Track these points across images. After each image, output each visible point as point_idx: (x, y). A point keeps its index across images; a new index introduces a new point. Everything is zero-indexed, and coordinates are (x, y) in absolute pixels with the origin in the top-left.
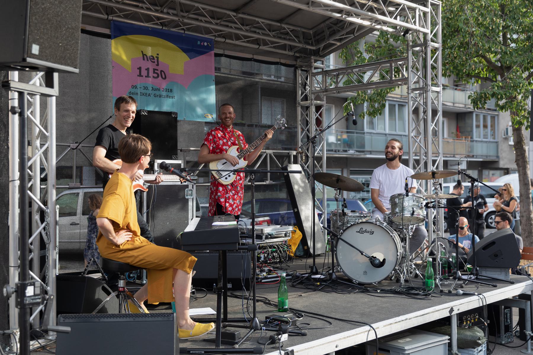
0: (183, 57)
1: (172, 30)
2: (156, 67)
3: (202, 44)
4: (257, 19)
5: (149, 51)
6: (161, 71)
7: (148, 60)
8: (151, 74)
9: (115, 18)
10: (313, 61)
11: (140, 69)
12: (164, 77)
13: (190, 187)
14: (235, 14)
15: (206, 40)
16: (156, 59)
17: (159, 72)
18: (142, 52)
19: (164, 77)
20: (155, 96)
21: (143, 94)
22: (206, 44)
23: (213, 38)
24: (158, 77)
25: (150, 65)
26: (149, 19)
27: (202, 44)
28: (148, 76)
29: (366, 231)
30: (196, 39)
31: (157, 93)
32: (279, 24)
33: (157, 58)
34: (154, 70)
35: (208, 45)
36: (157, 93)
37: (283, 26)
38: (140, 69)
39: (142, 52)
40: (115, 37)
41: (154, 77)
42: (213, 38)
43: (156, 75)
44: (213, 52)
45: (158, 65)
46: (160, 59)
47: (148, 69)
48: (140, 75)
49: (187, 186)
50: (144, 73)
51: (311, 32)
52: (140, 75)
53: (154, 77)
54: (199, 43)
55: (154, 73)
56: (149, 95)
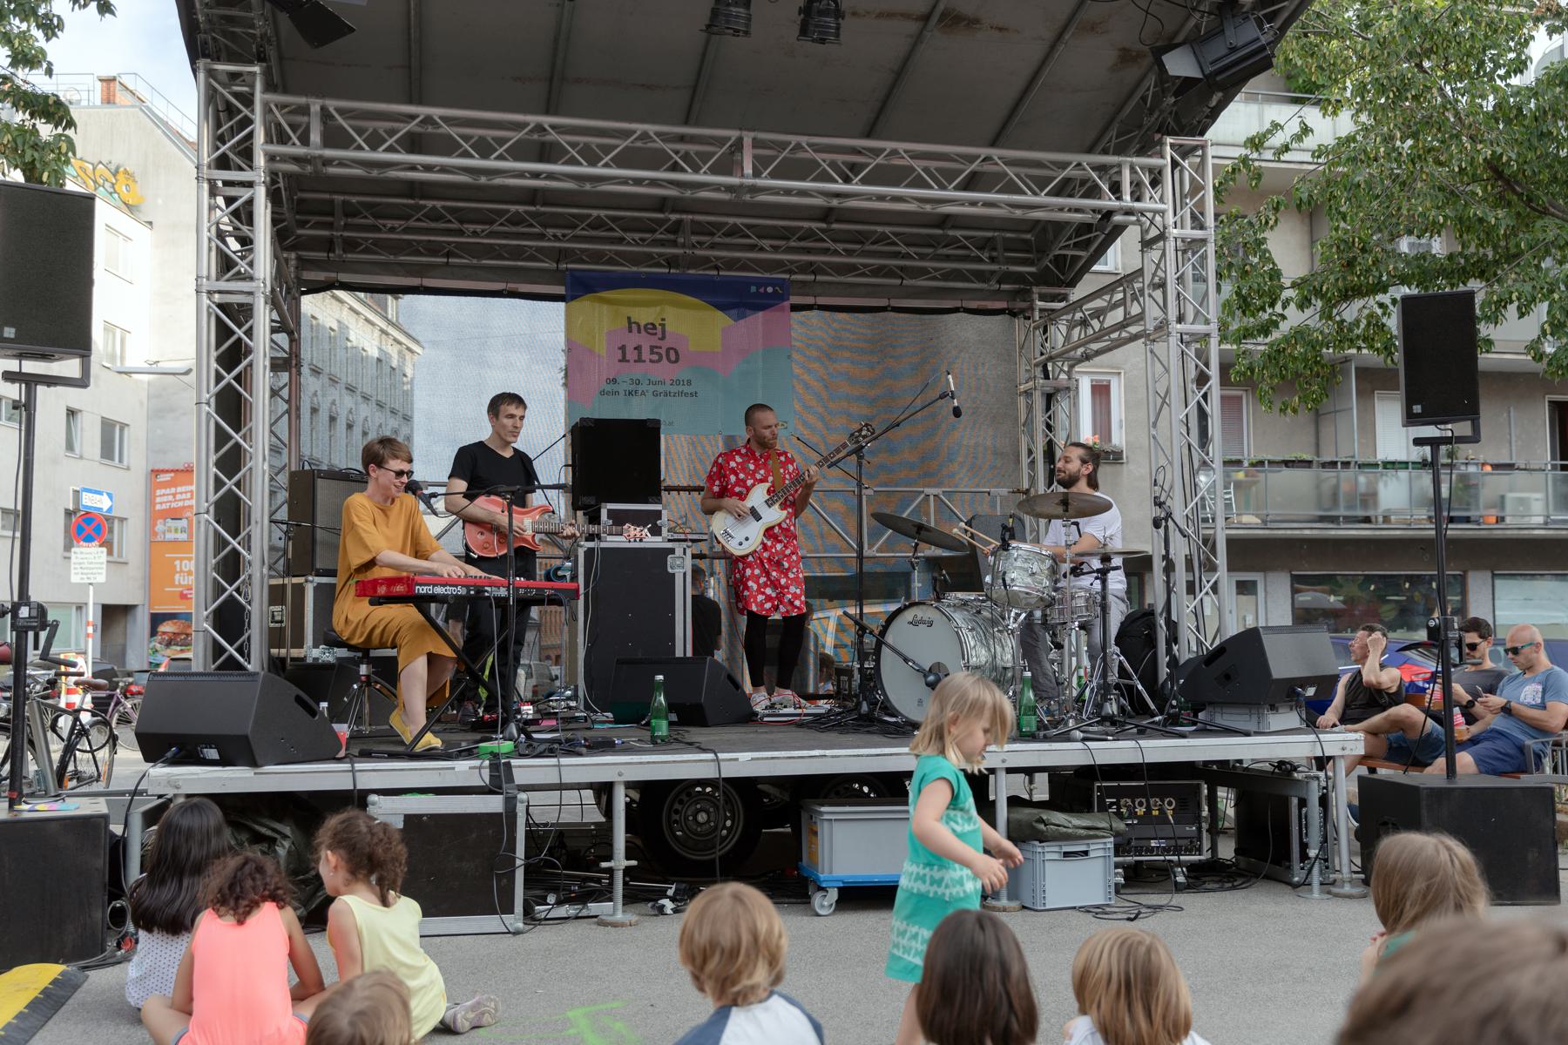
0: (721, 319)
1: (691, 272)
2: (659, 343)
3: (762, 290)
4: (880, 229)
5: (644, 316)
6: (668, 350)
7: (639, 331)
8: (646, 354)
9: (570, 266)
10: (1036, 296)
11: (623, 348)
12: (673, 358)
13: (679, 552)
14: (824, 225)
15: (772, 282)
16: (659, 328)
17: (663, 352)
18: (629, 318)
19: (673, 358)
20: (655, 394)
21: (630, 393)
22: (770, 290)
23: (787, 276)
24: (660, 360)
25: (646, 341)
26: (647, 259)
27: (762, 290)
28: (639, 360)
29: (922, 622)
30: (748, 282)
31: (660, 388)
32: (939, 232)
33: (663, 326)
34: (652, 348)
35: (775, 291)
36: (660, 388)
37: (951, 233)
38: (623, 348)
39: (629, 318)
40: (574, 298)
41: (651, 361)
42: (787, 276)
43: (655, 357)
44: (787, 304)
45: (663, 338)
46: (668, 328)
47: (638, 348)
48: (624, 359)
49: (672, 551)
50: (631, 355)
51: (1028, 236)
52: (624, 359)
53: (651, 361)
54: (753, 289)
55: (652, 352)
56: (643, 393)
